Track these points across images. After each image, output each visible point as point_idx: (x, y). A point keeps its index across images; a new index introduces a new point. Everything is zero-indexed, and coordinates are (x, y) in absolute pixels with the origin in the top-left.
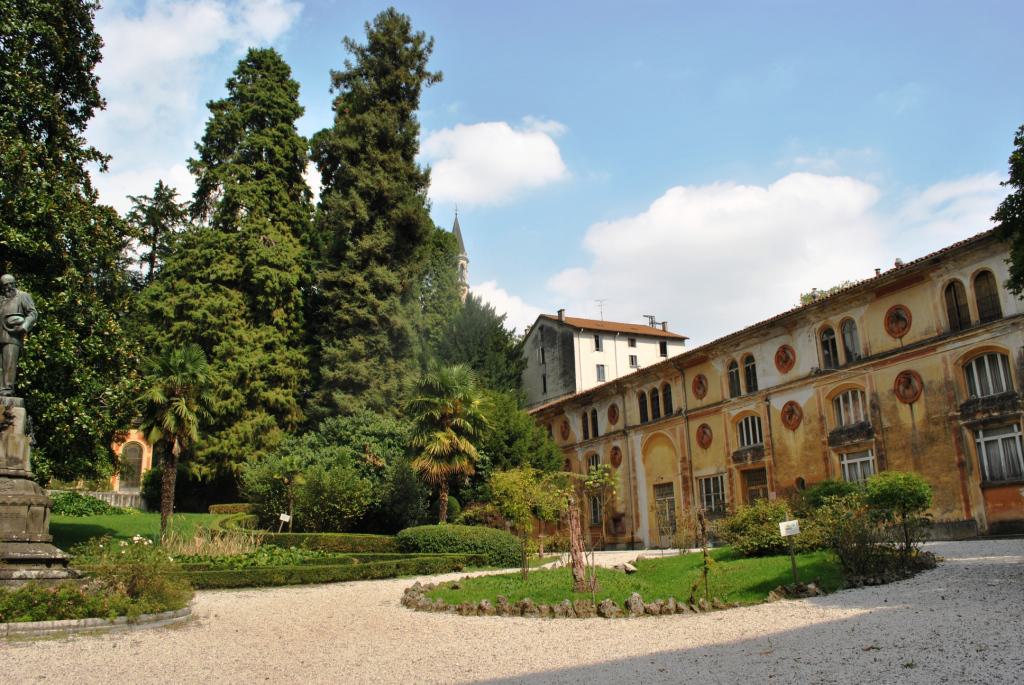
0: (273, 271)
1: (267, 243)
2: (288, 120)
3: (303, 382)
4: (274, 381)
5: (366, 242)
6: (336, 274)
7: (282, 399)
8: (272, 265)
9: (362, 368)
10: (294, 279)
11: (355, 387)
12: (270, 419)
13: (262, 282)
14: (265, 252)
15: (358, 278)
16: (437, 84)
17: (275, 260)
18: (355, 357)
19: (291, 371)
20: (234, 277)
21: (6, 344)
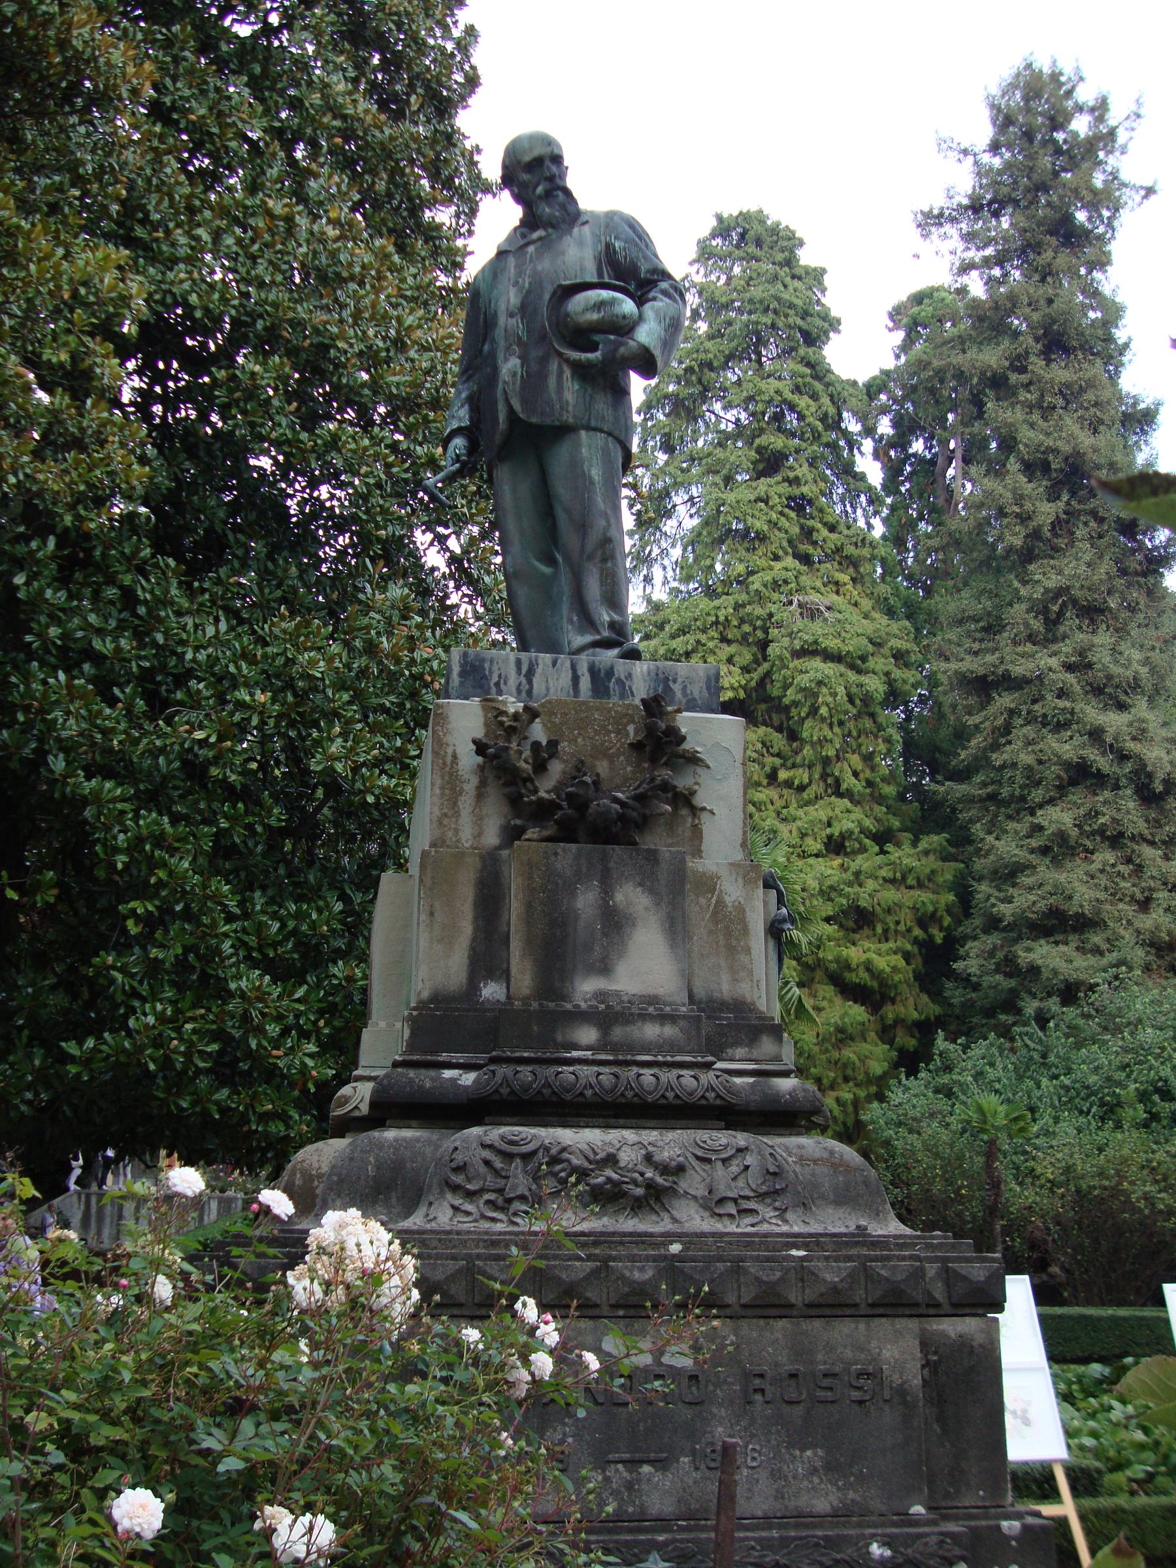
0: (829, 669)
1: (811, 613)
2: (813, 339)
3: (925, 920)
4: (858, 920)
5: (1047, 576)
6: (990, 658)
7: (882, 964)
8: (830, 656)
9: (1078, 884)
10: (875, 685)
11: (1058, 923)
12: (857, 1012)
13: (810, 693)
14: (815, 630)
15: (1047, 661)
16: (1153, 198)
17: (832, 644)
18: (1059, 849)
19: (891, 895)
20: (742, 695)
21: (563, 431)
